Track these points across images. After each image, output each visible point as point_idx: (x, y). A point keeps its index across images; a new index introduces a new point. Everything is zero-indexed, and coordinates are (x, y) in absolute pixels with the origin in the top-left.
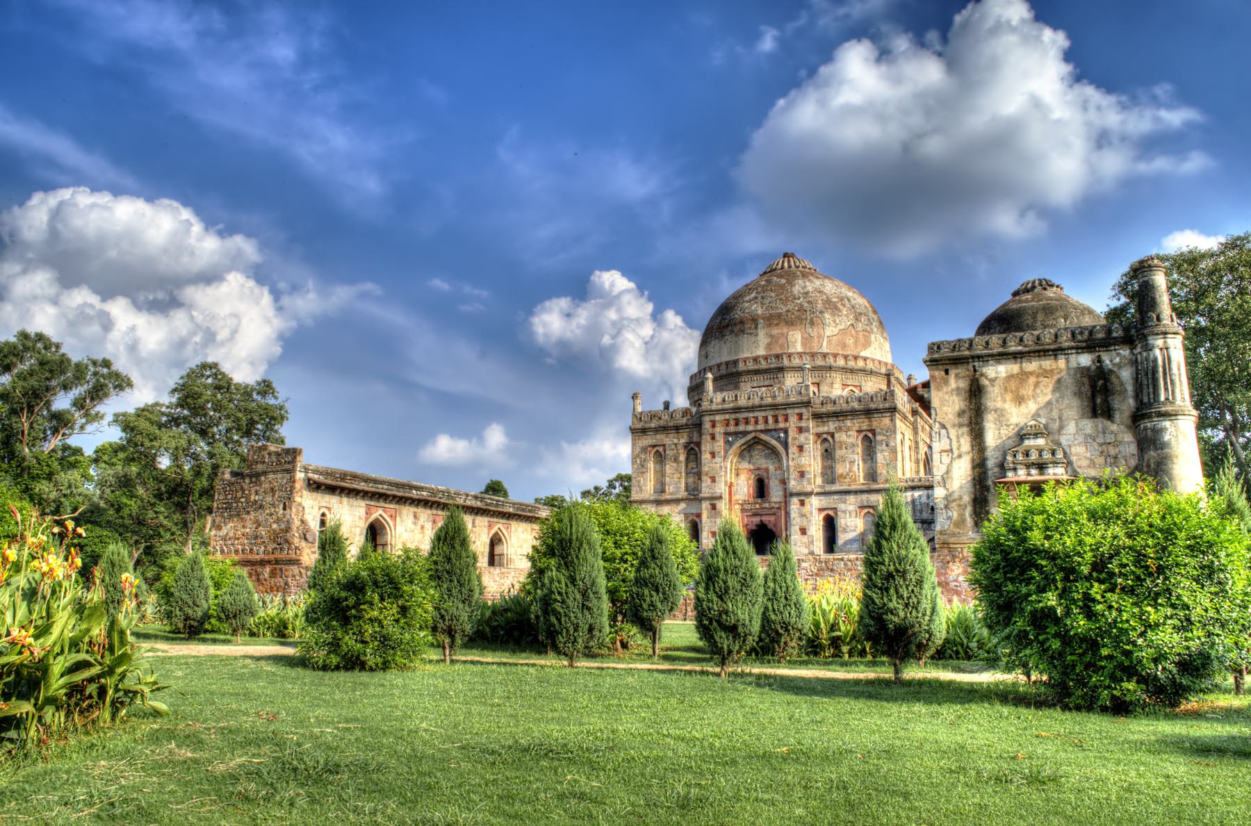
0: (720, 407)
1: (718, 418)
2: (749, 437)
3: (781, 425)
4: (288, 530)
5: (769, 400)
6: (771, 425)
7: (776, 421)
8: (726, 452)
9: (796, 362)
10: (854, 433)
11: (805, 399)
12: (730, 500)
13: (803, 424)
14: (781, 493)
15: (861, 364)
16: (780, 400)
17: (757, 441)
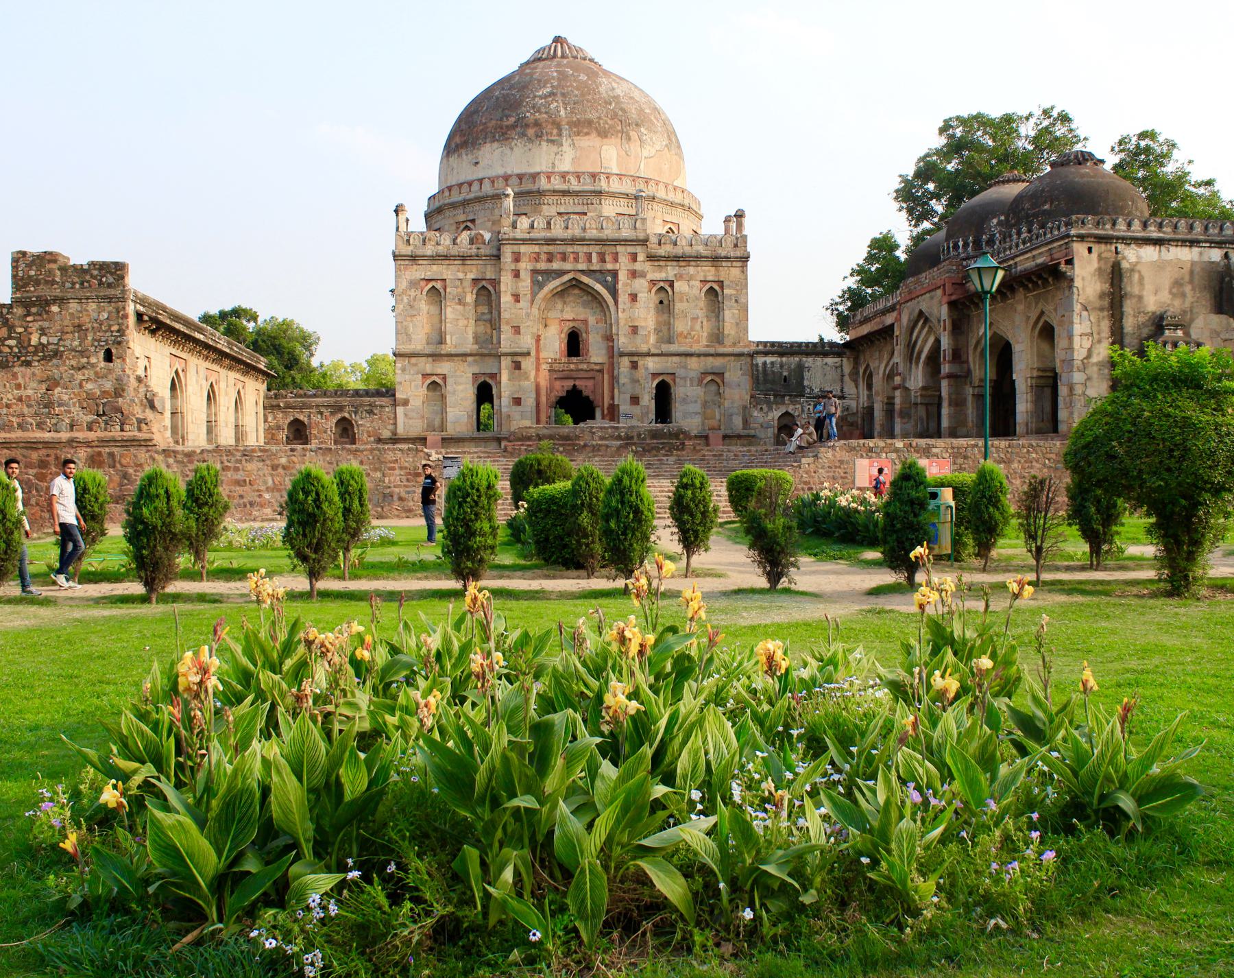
0: (527, 236)
1: (523, 249)
2: (566, 278)
3: (609, 266)
4: (119, 391)
5: (593, 233)
6: (596, 267)
7: (603, 260)
8: (534, 295)
9: (615, 186)
10: (697, 284)
11: (641, 236)
12: (538, 359)
13: (638, 266)
14: (604, 352)
15: (678, 198)
16: (609, 232)
17: (575, 284)
